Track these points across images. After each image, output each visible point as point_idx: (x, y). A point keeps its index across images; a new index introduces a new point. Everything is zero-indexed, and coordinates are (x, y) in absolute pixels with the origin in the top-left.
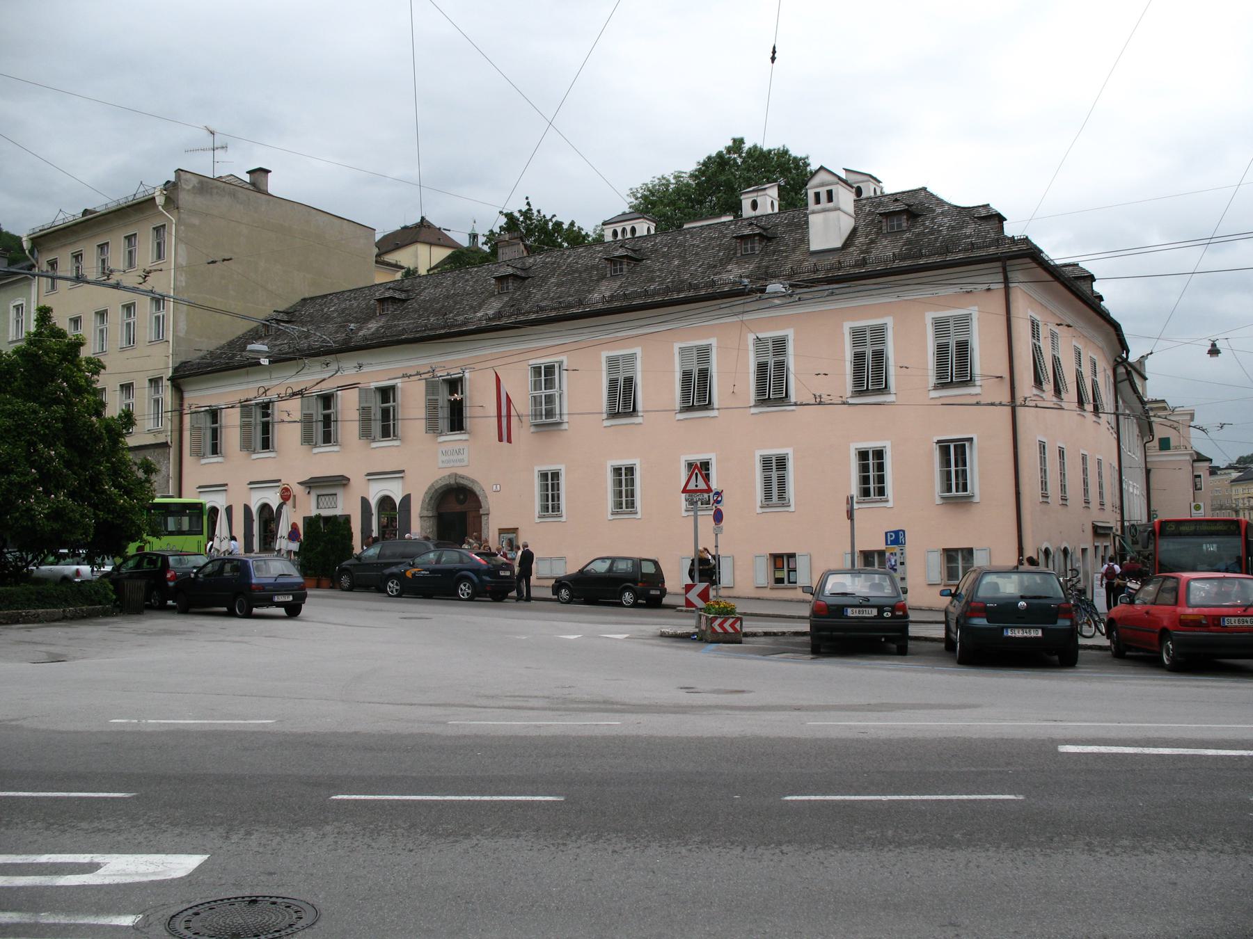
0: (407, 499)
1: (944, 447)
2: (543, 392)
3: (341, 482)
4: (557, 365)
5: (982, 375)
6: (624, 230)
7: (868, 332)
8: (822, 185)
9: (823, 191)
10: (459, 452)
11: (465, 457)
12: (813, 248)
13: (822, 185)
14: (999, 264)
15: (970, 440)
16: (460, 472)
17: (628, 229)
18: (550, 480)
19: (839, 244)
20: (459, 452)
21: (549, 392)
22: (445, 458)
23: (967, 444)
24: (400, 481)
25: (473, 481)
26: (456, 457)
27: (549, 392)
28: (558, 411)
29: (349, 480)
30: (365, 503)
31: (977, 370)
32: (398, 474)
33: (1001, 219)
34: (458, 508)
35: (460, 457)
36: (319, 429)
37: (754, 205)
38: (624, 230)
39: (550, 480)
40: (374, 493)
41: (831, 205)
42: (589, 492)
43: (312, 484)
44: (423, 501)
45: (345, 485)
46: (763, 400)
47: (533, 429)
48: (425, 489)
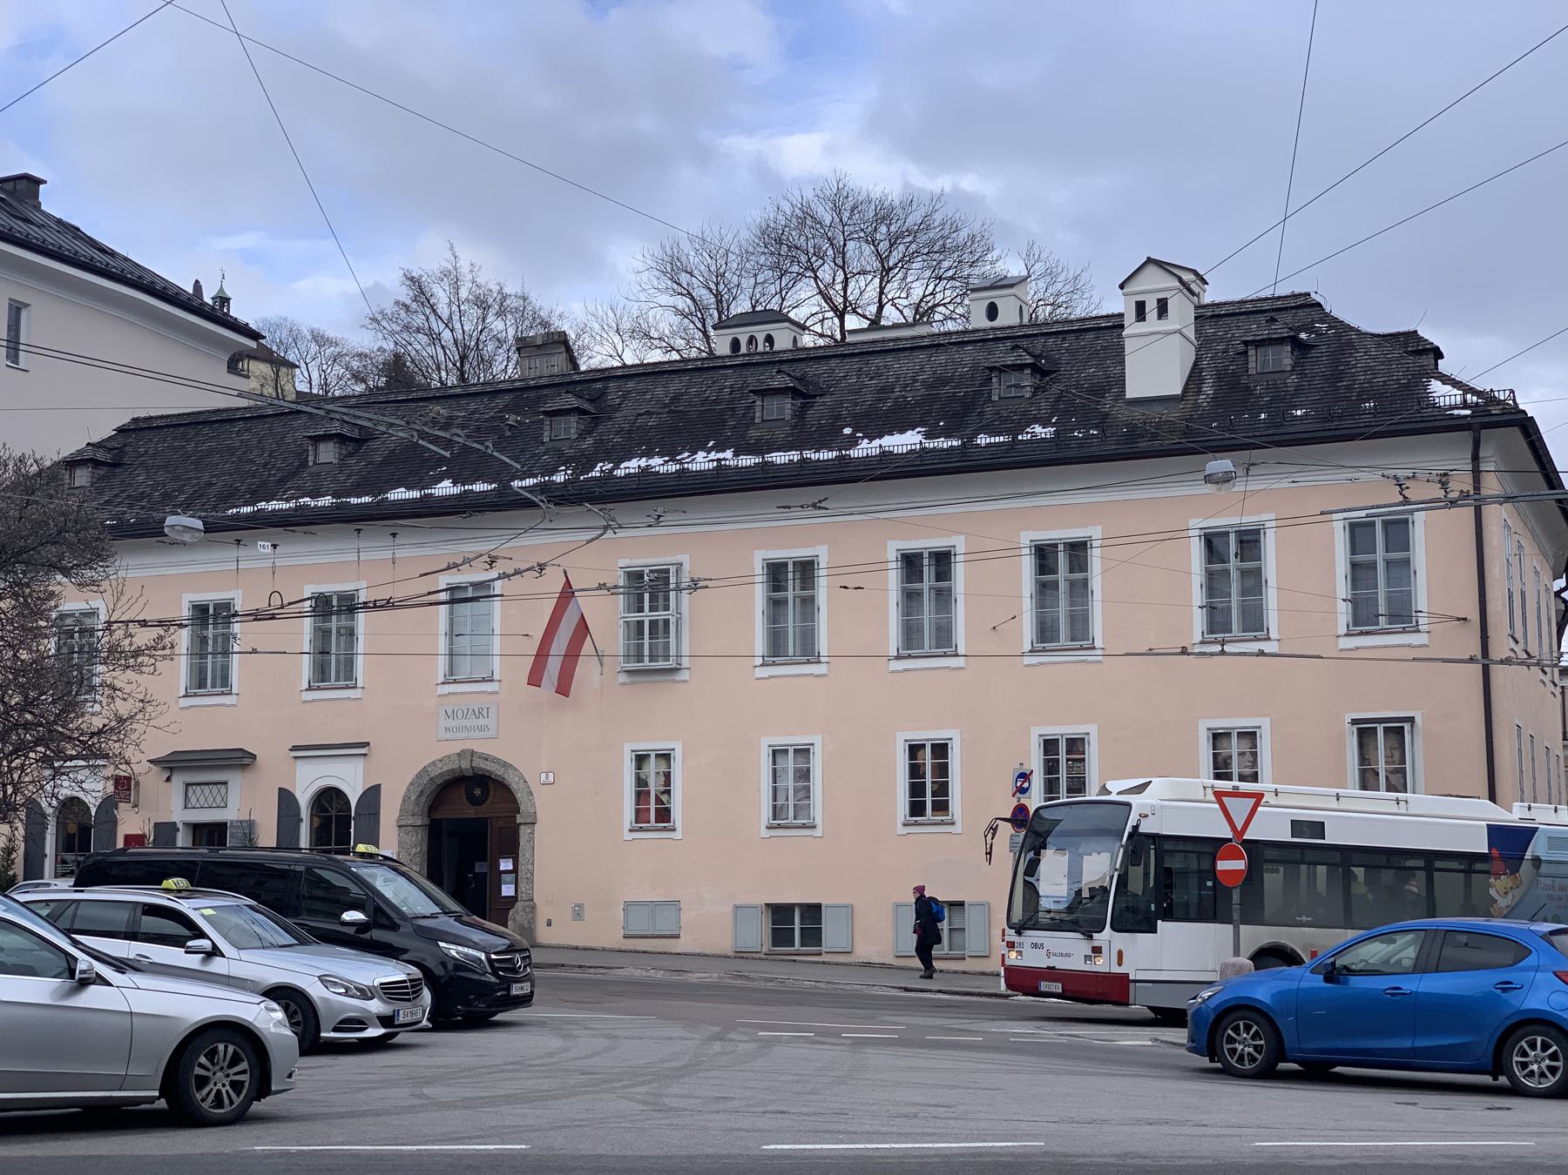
0: (372, 795)
1: (1365, 732)
2: (647, 616)
3: (240, 760)
4: (672, 569)
5: (1431, 615)
6: (752, 340)
7: (1232, 537)
10: (479, 714)
11: (490, 722)
12: (1132, 392)
14: (1467, 436)
15: (1411, 720)
17: (761, 338)
19: (1178, 391)
20: (479, 714)
21: (660, 615)
22: (451, 723)
23: (1407, 727)
24: (360, 762)
25: (506, 765)
27: (660, 615)
28: (673, 652)
29: (254, 757)
30: (286, 799)
31: (1421, 601)
32: (357, 748)
33: (1441, 356)
34: (470, 812)
35: (482, 722)
37: (992, 312)
38: (752, 340)
40: (307, 782)
42: (720, 789)
43: (172, 764)
44: (406, 799)
45: (244, 767)
47: (623, 678)
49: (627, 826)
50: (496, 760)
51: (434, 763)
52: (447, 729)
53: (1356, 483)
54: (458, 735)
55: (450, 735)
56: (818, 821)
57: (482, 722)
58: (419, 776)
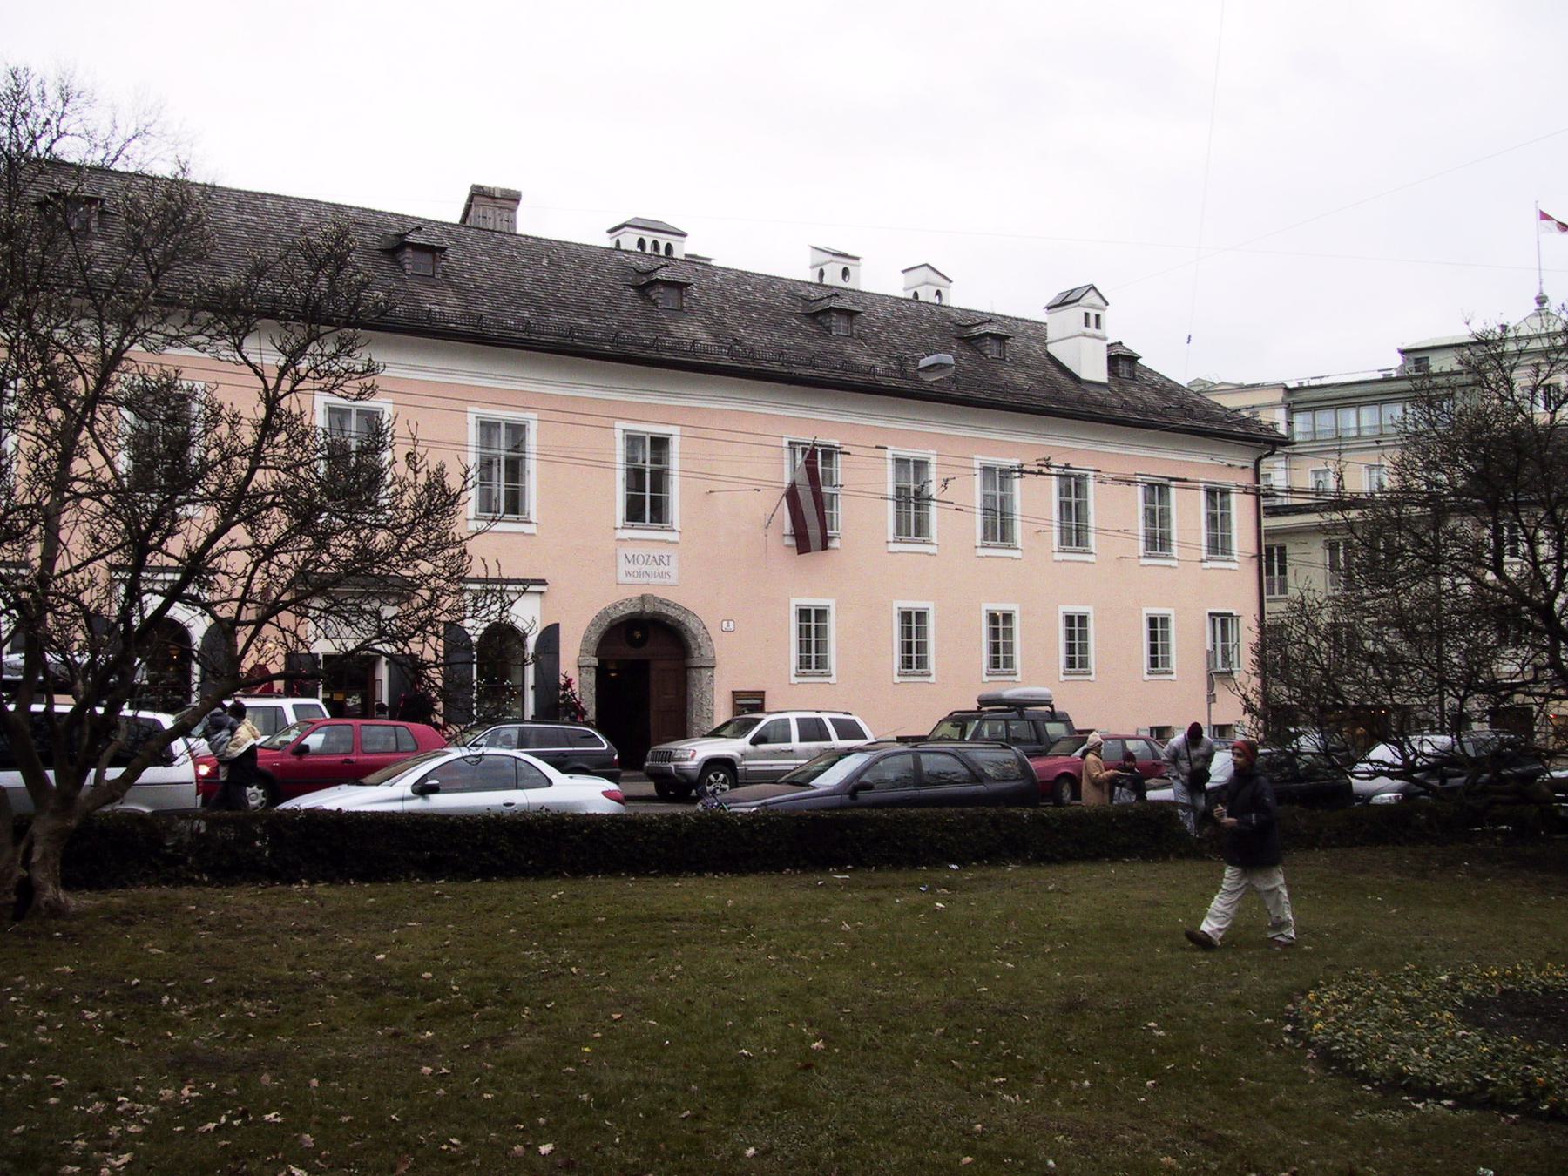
0: (550, 636)
6: (656, 244)
8: (1093, 307)
9: (1092, 313)
10: (660, 561)
11: (673, 569)
13: (1093, 307)
16: (661, 594)
18: (812, 622)
20: (660, 561)
22: (631, 568)
25: (686, 611)
26: (653, 568)
34: (632, 654)
35: (662, 569)
36: (500, 485)
38: (656, 244)
39: (812, 622)
41: (1098, 332)
46: (634, 512)
48: (591, 616)
49: (793, 672)
50: (677, 607)
51: (615, 607)
52: (628, 574)
53: (1010, 443)
54: (638, 580)
55: (630, 579)
56: (932, 671)
57: (662, 569)
58: (599, 617)
